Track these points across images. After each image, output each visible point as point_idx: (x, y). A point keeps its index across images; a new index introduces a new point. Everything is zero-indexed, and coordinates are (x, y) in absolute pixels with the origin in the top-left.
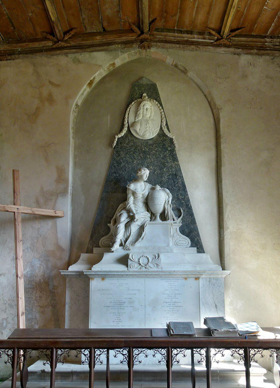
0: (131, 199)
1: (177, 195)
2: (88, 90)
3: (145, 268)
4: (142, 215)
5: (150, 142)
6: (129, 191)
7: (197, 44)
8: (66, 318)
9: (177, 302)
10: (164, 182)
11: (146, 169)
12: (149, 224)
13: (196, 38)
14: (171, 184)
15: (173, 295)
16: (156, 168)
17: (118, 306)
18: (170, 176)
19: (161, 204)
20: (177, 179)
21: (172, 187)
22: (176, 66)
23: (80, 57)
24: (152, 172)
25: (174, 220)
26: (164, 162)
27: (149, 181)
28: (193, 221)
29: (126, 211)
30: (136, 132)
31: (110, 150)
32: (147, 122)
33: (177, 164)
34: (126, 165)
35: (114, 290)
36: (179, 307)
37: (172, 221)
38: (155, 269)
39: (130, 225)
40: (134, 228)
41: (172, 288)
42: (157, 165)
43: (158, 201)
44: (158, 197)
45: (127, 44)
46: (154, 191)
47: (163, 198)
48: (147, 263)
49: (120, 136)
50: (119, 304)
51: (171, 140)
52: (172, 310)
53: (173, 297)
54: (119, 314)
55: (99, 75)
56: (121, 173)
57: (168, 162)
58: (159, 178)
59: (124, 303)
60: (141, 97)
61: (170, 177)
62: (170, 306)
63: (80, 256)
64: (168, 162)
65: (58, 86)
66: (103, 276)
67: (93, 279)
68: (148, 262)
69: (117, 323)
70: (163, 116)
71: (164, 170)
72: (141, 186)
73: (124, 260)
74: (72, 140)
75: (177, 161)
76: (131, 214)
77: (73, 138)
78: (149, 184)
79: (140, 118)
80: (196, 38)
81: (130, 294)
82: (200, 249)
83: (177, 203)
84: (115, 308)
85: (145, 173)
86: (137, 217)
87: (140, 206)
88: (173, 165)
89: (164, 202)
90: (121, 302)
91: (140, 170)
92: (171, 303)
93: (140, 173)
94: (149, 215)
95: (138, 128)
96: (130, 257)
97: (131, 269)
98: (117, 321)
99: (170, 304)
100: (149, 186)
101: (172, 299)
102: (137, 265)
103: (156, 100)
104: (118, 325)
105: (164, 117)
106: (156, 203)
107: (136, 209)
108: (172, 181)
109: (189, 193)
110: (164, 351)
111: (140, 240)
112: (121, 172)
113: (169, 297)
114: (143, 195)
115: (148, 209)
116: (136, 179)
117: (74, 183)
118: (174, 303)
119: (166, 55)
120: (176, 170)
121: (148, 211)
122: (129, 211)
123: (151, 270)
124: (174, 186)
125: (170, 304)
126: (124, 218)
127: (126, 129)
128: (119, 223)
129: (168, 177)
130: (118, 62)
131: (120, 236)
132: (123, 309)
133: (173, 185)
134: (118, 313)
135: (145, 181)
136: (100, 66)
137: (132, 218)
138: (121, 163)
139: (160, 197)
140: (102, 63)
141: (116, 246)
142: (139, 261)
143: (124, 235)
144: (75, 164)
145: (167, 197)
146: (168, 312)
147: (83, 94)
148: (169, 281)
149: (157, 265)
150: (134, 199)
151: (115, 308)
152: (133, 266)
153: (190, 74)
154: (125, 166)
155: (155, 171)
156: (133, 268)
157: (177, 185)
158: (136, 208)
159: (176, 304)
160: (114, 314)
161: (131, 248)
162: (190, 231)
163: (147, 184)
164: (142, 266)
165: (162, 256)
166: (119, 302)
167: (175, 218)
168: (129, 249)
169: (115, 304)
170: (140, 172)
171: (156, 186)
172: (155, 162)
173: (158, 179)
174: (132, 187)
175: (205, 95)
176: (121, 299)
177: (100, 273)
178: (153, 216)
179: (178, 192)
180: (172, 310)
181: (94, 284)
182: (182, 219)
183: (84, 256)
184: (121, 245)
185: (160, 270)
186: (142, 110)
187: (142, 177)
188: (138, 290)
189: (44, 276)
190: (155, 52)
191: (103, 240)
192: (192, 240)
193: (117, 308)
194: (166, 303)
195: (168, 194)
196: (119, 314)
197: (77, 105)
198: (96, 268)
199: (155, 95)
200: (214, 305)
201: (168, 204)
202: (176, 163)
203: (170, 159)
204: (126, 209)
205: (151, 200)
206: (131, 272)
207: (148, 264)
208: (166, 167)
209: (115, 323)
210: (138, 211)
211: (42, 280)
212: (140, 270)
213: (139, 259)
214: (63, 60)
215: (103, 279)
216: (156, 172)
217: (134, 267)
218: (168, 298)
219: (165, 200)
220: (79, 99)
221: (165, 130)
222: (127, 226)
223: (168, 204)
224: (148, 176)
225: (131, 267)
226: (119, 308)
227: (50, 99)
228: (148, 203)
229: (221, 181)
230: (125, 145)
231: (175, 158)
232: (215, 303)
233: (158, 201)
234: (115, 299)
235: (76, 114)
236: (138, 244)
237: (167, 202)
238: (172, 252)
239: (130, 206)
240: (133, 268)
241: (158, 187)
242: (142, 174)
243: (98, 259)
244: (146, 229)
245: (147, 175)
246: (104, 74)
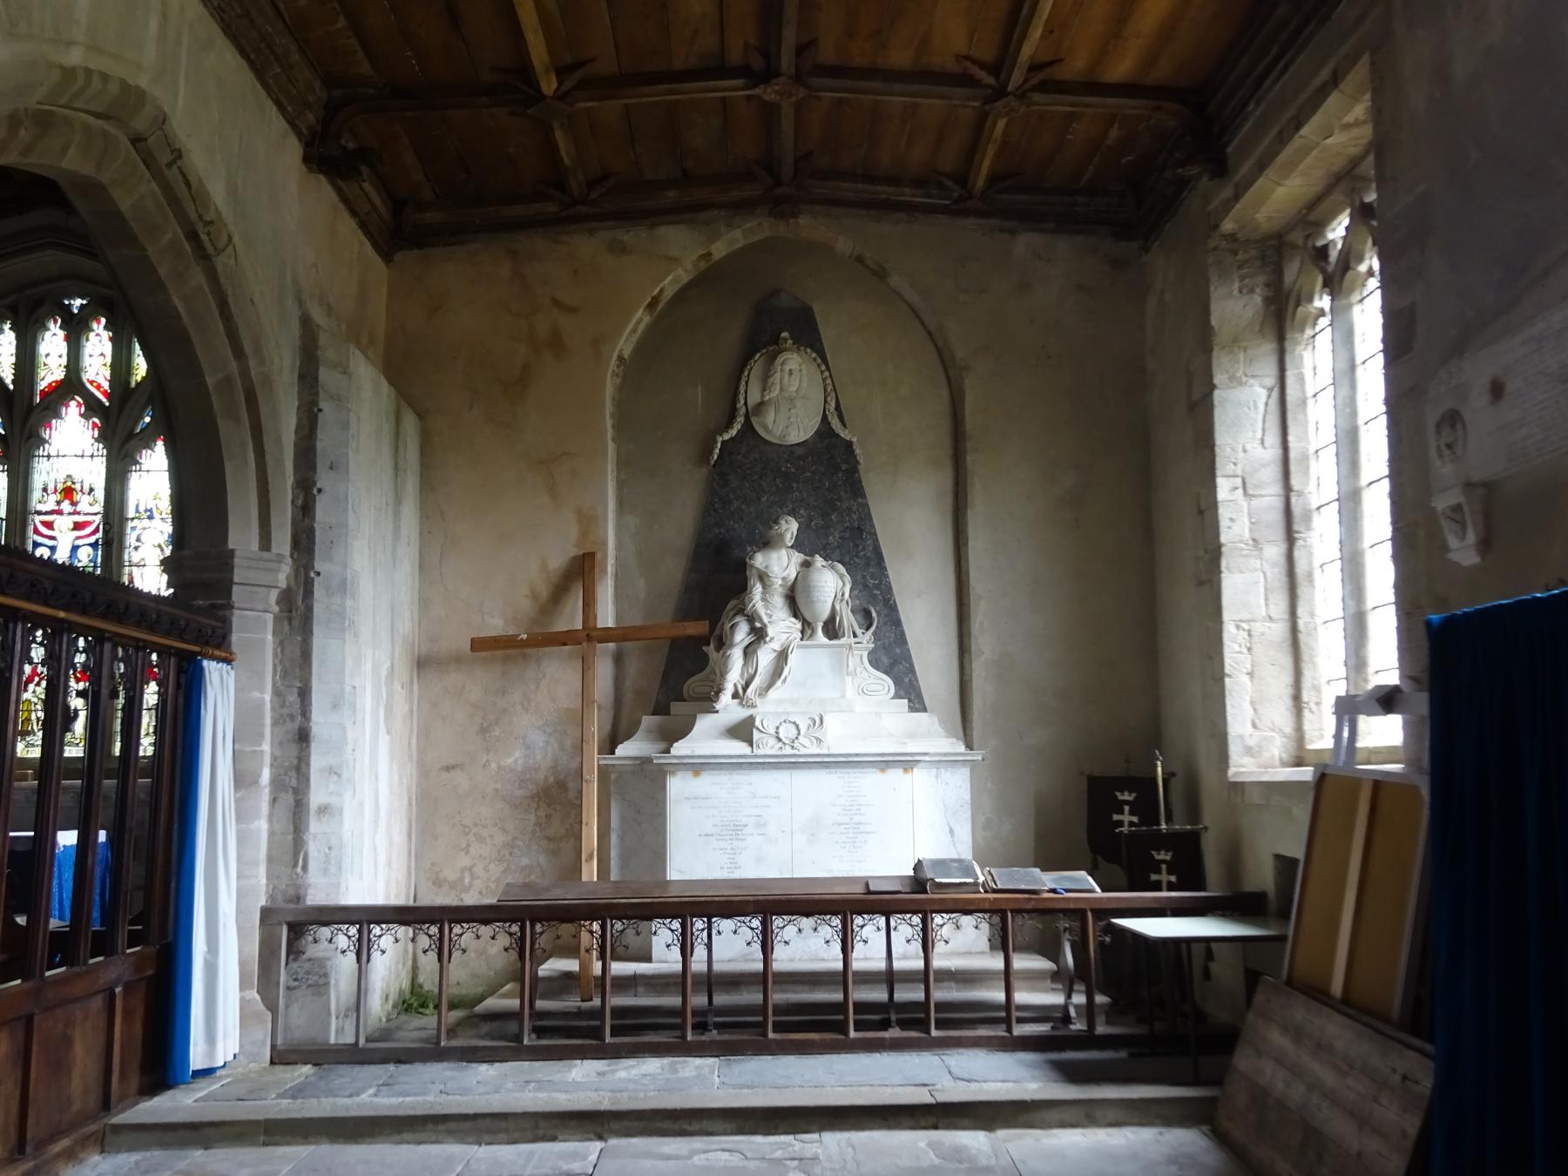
1: (864, 577)
2: (647, 319)
4: (781, 626)
5: (800, 451)
7: (910, 208)
8: (613, 862)
12: (799, 646)
13: (908, 195)
22: (860, 259)
23: (626, 238)
25: (855, 636)
27: (798, 546)
28: (901, 639)
30: (766, 428)
31: (704, 471)
32: (791, 401)
37: (853, 640)
38: (814, 750)
39: (755, 652)
40: (765, 656)
45: (742, 207)
47: (831, 585)
49: (727, 437)
51: (850, 444)
55: (671, 283)
57: (840, 499)
60: (776, 340)
63: (639, 723)
64: (840, 499)
65: (573, 310)
66: (698, 767)
67: (673, 773)
70: (830, 388)
73: (743, 731)
74: (611, 446)
75: (863, 496)
76: (758, 625)
77: (614, 440)
79: (774, 395)
80: (908, 195)
82: (917, 703)
86: (771, 631)
91: (776, 522)
94: (799, 626)
95: (770, 417)
96: (758, 723)
100: (798, 557)
102: (772, 741)
103: (813, 349)
105: (831, 389)
109: (890, 572)
110: (836, 921)
111: (779, 683)
114: (784, 579)
115: (795, 612)
116: (766, 544)
117: (619, 547)
119: (840, 236)
121: (795, 616)
122: (751, 618)
123: (804, 751)
126: (741, 635)
127: (740, 420)
128: (731, 646)
130: (720, 250)
131: (734, 676)
136: (674, 261)
137: (759, 634)
140: (676, 256)
141: (726, 698)
143: (742, 675)
144: (621, 502)
147: (634, 331)
149: (819, 740)
153: (895, 280)
161: (758, 701)
162: (893, 659)
165: (827, 720)
167: (859, 632)
168: (753, 706)
174: (759, 560)
175: (930, 334)
178: (807, 628)
181: (677, 786)
182: (874, 634)
183: (647, 721)
184: (735, 696)
186: (778, 375)
187: (781, 536)
189: (554, 767)
190: (808, 226)
191: (692, 685)
192: (898, 682)
195: (841, 577)
197: (620, 358)
198: (680, 748)
199: (808, 337)
211: (551, 779)
214: (587, 245)
217: (767, 746)
220: (625, 344)
221: (835, 423)
222: (749, 652)
227: (556, 343)
228: (795, 600)
229: (966, 543)
230: (739, 458)
231: (857, 491)
235: (618, 381)
236: (773, 694)
238: (852, 710)
241: (819, 561)
243: (683, 731)
244: (792, 658)
246: (685, 279)
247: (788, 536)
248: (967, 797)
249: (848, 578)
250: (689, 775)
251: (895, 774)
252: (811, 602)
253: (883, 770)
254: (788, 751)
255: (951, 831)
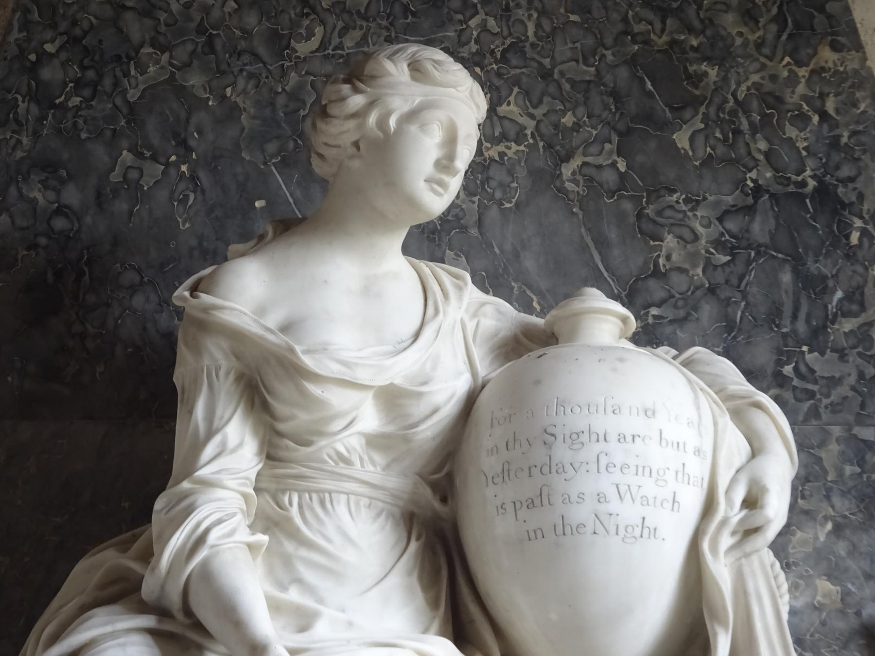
0: (227, 460)
6: (197, 350)
10: (679, 282)
11: (440, 55)
14: (774, 316)
16: (568, 120)
18: (750, 210)
19: (646, 530)
20: (850, 255)
21: (782, 356)
24: (521, 172)
26: (673, 43)
29: (148, 621)
33: (841, 77)
34: (195, 81)
42: (584, 87)
43: (605, 484)
44: (601, 423)
46: (551, 351)
56: (115, 177)
57: (720, 52)
58: (613, 235)
61: (760, 229)
64: (720, 52)
71: (682, 139)
72: (369, 290)
78: (473, 293)
83: (853, 551)
85: (435, 115)
87: (349, 555)
88: (793, 80)
89: (692, 502)
91: (357, 73)
93: (360, 115)
106: (581, 513)
107: (294, 595)
108: (786, 277)
112: (127, 156)
114: (392, 398)
116: (292, 196)
120: (834, 143)
124: (817, 338)
129: (732, 225)
133: (801, 327)
135: (430, 242)
138: (127, 57)
139: (631, 423)
145: (735, 445)
150: (270, 454)
154: (181, 91)
155: (567, 158)
157: (848, 325)
158: (299, 581)
163: (460, 289)
170: (357, 101)
171: (576, 305)
172: (563, 50)
173: (602, 244)
174: (249, 292)
179: (860, 420)
187: (382, 151)
201: (749, 532)
202: (827, 56)
203: (749, 16)
204: (148, 589)
205: (506, 473)
208: (694, 103)
210: (321, 629)
216: (567, 171)
219: (699, 470)
223: (749, 532)
224: (465, 155)
233: (605, 484)
237: (730, 510)
239: (201, 541)
241: (604, 319)
242: (382, 123)
245: (451, 141)
247: (423, 152)
249: (775, 422)
252: (551, 536)
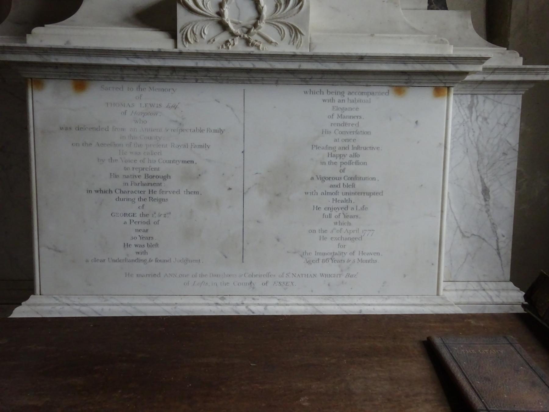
3: (243, 42)
9: (360, 179)
15: (351, 152)
17: (141, 188)
35: (123, 130)
36: (369, 194)
38: (285, 48)
41: (345, 124)
48: (253, 21)
50: (145, 181)
52: (344, 205)
53: (347, 159)
54: (146, 219)
59: (165, 178)
62: (336, 193)
66: (84, 71)
67: (38, 83)
68: (259, 17)
69: (139, 249)
81: (186, 146)
84: (131, 196)
90: (151, 173)
92: (342, 182)
97: (187, 45)
98: (138, 241)
99: (336, 182)
101: (343, 166)
102: (210, 30)
104: (143, 257)
113: (333, 160)
118: (350, 182)
125: (336, 182)
132: (161, 200)
134: (143, 215)
142: (220, 14)
146: (327, 213)
148: (337, 98)
149: (295, 31)
151: (131, 196)
152: (198, 34)
156: (195, 41)
159: (358, 183)
160: (127, 219)
164: (233, 35)
166: (147, 176)
169: (129, 181)
176: (154, 166)
177: (63, 59)
180: (344, 205)
181: (46, 105)
185: (304, 50)
188: (215, 131)
193: (138, 196)
194: (323, 179)
196: (146, 219)
200: (480, 188)
206: (188, 58)
207: (255, 25)
209: (132, 251)
212: (224, 50)
213: (221, 5)
215: (80, 86)
217: (202, 38)
218: (330, 163)
225: (187, 39)
226: (146, 195)
232: (482, 180)
234: (130, 165)
240: (195, 41)
248: (514, 140)
250: (67, 87)
251: (420, 98)
253: (399, 90)
254: (238, 46)
255: (486, 191)
